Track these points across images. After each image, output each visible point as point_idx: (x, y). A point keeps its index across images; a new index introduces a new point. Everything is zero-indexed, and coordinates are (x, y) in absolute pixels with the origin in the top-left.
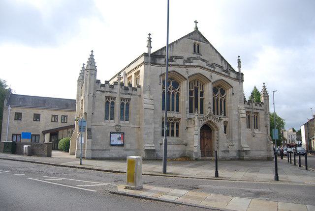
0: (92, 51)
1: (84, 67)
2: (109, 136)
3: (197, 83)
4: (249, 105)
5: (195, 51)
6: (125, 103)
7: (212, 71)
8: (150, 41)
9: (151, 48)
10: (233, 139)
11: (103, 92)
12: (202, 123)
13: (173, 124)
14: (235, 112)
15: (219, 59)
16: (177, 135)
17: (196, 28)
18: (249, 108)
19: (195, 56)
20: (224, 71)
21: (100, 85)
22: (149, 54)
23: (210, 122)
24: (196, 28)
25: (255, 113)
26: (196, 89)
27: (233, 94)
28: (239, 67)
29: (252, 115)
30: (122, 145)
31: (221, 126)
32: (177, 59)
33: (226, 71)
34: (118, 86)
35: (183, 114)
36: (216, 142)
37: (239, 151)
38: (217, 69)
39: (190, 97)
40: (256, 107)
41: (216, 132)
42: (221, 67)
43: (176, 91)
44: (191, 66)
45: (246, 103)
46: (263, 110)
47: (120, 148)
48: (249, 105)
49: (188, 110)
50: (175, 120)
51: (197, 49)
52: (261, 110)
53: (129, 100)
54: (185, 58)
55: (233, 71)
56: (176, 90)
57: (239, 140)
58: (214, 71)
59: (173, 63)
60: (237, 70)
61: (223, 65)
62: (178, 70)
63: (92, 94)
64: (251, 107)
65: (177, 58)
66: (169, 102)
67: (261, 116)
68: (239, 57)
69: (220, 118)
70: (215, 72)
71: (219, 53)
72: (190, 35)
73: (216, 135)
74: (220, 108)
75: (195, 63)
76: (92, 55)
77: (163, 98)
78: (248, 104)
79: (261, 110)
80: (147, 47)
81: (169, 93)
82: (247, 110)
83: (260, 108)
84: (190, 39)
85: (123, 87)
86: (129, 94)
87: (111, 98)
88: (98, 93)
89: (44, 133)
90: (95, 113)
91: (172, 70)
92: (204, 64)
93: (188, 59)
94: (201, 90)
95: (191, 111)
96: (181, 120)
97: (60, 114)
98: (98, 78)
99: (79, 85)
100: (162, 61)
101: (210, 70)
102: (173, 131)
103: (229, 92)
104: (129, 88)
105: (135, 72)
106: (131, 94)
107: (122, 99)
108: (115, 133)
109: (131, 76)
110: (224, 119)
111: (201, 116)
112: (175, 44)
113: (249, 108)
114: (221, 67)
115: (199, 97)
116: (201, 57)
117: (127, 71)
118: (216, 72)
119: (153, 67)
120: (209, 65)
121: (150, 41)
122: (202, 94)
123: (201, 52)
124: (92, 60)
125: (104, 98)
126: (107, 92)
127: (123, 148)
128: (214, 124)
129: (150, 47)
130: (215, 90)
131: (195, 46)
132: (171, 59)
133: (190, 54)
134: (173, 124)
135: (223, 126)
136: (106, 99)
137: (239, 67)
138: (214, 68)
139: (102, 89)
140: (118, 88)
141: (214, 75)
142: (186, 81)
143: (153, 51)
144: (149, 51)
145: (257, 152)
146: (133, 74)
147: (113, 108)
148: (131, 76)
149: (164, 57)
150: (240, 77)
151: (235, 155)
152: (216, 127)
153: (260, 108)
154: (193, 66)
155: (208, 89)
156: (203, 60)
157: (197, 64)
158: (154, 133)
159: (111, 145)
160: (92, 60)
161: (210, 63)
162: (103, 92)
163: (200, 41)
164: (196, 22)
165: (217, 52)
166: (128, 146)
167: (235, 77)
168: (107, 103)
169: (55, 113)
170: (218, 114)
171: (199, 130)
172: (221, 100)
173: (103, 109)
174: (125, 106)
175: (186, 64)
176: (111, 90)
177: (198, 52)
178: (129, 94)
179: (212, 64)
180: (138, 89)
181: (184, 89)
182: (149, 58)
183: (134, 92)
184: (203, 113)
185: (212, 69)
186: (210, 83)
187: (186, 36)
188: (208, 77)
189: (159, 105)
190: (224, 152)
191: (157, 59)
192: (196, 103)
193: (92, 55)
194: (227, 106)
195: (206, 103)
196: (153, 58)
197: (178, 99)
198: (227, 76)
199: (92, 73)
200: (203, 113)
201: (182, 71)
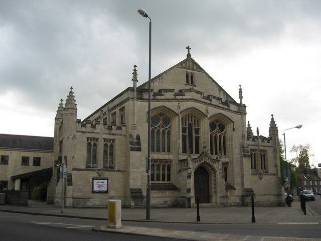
0: (72, 88)
1: (61, 104)
2: (91, 181)
3: (192, 117)
4: (254, 141)
5: (187, 82)
6: (109, 144)
7: (209, 104)
8: (135, 73)
9: (137, 81)
10: (235, 182)
11: (84, 132)
13: (164, 166)
14: (237, 151)
15: (216, 89)
16: (169, 179)
17: (189, 55)
18: (254, 145)
19: (188, 87)
20: (223, 103)
21: (80, 124)
22: (135, 89)
23: (205, 163)
24: (189, 55)
26: (190, 126)
28: (241, 97)
30: (106, 192)
31: (218, 167)
32: (167, 92)
33: (225, 103)
35: (175, 155)
36: (213, 186)
37: (243, 196)
38: (214, 102)
39: (182, 135)
40: (263, 144)
41: (213, 175)
42: (219, 99)
43: (166, 129)
44: (183, 99)
45: (251, 139)
47: (103, 195)
48: (254, 141)
49: (181, 150)
50: (166, 161)
51: (190, 80)
52: (269, 147)
53: (113, 140)
54: (177, 91)
55: (234, 102)
56: (167, 127)
57: (243, 184)
58: (210, 104)
59: (162, 97)
60: (238, 101)
61: (222, 96)
62: (167, 104)
63: (72, 137)
64: (257, 143)
65: (167, 91)
66: (158, 141)
67: (270, 154)
68: (240, 86)
69: (217, 158)
70: (212, 105)
72: (181, 63)
73: (213, 178)
74: (219, 145)
76: (71, 92)
78: (254, 140)
79: (269, 147)
81: (158, 131)
83: (268, 144)
86: (113, 134)
88: (78, 134)
89: (14, 179)
90: (76, 156)
92: (198, 97)
93: (180, 91)
95: (184, 151)
96: (173, 162)
97: (31, 155)
98: (78, 118)
99: (56, 124)
102: (163, 175)
103: (229, 128)
104: (113, 127)
105: (119, 108)
107: (105, 140)
108: (97, 179)
109: (115, 113)
110: (223, 159)
111: (195, 156)
112: (164, 75)
113: (254, 145)
114: (219, 99)
115: (194, 135)
116: (195, 88)
117: (111, 106)
118: (215, 105)
120: (205, 98)
121: (135, 73)
122: (197, 131)
124: (71, 98)
126: (89, 132)
127: (106, 195)
128: (210, 166)
129: (135, 80)
130: (212, 126)
131: (187, 76)
132: (160, 92)
133: (182, 86)
135: (220, 167)
136: (88, 140)
137: (241, 97)
138: (211, 100)
139: (83, 129)
140: (100, 128)
141: (210, 108)
142: (177, 117)
143: (138, 84)
144: (135, 84)
145: (264, 197)
146: (117, 110)
147: (95, 151)
148: (115, 113)
149: (148, 91)
150: (241, 109)
151: (238, 201)
152: (213, 169)
153: (268, 144)
154: (186, 99)
155: (205, 125)
156: (198, 92)
157: (191, 98)
158: (142, 177)
159: (94, 192)
160: (71, 98)
161: (206, 95)
162: (84, 132)
163: (193, 70)
165: (214, 81)
167: (236, 110)
168: (89, 144)
169: (26, 154)
170: (216, 154)
171: (193, 174)
172: (220, 137)
173: (85, 153)
174: (109, 147)
175: (178, 97)
176: (92, 130)
178: (113, 134)
179: (209, 96)
180: (123, 128)
181: (176, 127)
185: (208, 102)
186: (206, 119)
188: (204, 111)
189: (144, 145)
190: (223, 197)
192: (191, 142)
193: (71, 92)
194: (228, 143)
195: (201, 141)
196: (140, 92)
197: (169, 138)
198: (226, 109)
199: (71, 112)
201: (172, 105)
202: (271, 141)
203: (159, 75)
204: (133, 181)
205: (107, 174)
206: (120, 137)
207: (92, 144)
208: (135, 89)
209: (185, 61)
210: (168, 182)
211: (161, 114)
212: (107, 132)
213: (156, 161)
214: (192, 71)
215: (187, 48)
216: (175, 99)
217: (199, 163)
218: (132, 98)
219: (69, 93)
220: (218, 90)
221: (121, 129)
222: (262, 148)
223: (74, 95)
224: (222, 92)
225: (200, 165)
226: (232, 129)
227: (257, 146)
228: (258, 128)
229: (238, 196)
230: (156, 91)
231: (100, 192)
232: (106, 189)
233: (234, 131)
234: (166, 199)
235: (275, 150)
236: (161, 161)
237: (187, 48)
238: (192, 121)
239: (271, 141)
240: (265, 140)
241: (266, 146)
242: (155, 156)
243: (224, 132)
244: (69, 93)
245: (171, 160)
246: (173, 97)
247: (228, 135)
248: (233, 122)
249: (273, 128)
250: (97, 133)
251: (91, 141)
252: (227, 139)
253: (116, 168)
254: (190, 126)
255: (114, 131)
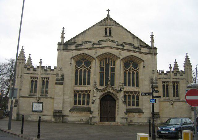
2: (32, 104)
5: (106, 34)
7: (121, 49)
9: (64, 38)
11: (28, 74)
12: (100, 94)
13: (84, 95)
15: (131, 37)
17: (108, 15)
18: (166, 78)
22: (62, 43)
24: (108, 15)
25: (173, 82)
26: (107, 65)
27: (144, 67)
28: (152, 41)
29: (171, 85)
30: (41, 112)
32: (86, 43)
34: (40, 69)
38: (126, 47)
40: (176, 77)
46: (185, 79)
50: (86, 91)
51: (108, 32)
52: (181, 79)
53: (48, 78)
55: (147, 46)
58: (123, 49)
59: (83, 47)
60: (150, 45)
62: (86, 52)
63: (20, 76)
64: (168, 76)
65: (86, 42)
71: (130, 33)
72: (101, 22)
75: (104, 44)
77: (76, 76)
79: (181, 79)
80: (61, 38)
82: (164, 80)
83: (181, 77)
84: (101, 25)
85: (43, 69)
86: (48, 74)
87: (35, 78)
90: (23, 89)
91: (82, 53)
92: (113, 45)
94: (113, 66)
100: (73, 47)
101: (119, 48)
103: (141, 65)
106: (49, 74)
107: (43, 78)
112: (87, 32)
113: (166, 78)
119: (65, 53)
122: (113, 69)
123: (112, 35)
125: (29, 79)
128: (114, 95)
129: (63, 37)
130: (126, 65)
131: (106, 31)
134: (84, 95)
137: (152, 41)
138: (124, 46)
139: (28, 72)
141: (122, 52)
142: (94, 60)
143: (65, 41)
144: (63, 40)
149: (74, 43)
150: (152, 51)
152: (116, 97)
153: (181, 77)
156: (112, 41)
157: (106, 45)
159: (33, 111)
162: (28, 74)
163: (110, 25)
164: (108, 10)
166: (45, 112)
168: (32, 81)
172: (133, 73)
174: (45, 83)
175: (95, 46)
177: (110, 34)
178: (48, 74)
181: (95, 67)
182: (62, 46)
183: (52, 72)
184: (138, 86)
185: (122, 47)
187: (97, 24)
188: (117, 54)
190: (122, 118)
191: (68, 46)
194: (140, 77)
197: (89, 76)
198: (137, 51)
199: (20, 61)
200: (138, 86)
201: (92, 53)
202: (183, 74)
203: (85, 31)
204: (56, 105)
205: (42, 100)
206: (52, 76)
207: (33, 83)
208: (62, 43)
209: (106, 19)
210: (87, 106)
211: (83, 59)
212: (44, 73)
213: (78, 91)
214: (110, 27)
215: (107, 10)
216: (93, 48)
217: (102, 93)
218: (60, 50)
219: (21, 49)
220: (132, 38)
221: (54, 71)
222: (175, 80)
223: (24, 51)
224: (136, 39)
225: (105, 93)
226: (143, 66)
227: (169, 78)
228: (170, 65)
229: (146, 118)
230: (80, 43)
231: (37, 111)
232: (41, 110)
233: (144, 68)
234: (82, 118)
235: (187, 81)
236: (82, 91)
237: (107, 10)
238: (109, 62)
239: (183, 74)
240: (178, 74)
241: (178, 79)
242: (78, 88)
243: (137, 69)
244: (21, 49)
245: (90, 91)
246: (92, 47)
247: (140, 72)
248: (143, 61)
249: (188, 63)
250: (37, 74)
251: (45, 79)
252: (140, 74)
253: (49, 96)
254: (107, 65)
255: (48, 72)
